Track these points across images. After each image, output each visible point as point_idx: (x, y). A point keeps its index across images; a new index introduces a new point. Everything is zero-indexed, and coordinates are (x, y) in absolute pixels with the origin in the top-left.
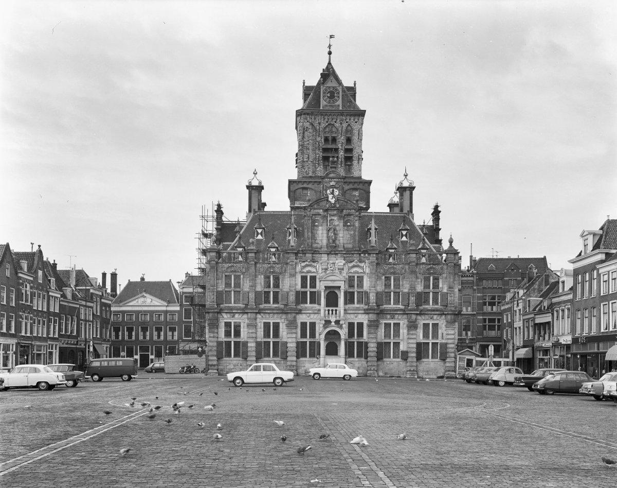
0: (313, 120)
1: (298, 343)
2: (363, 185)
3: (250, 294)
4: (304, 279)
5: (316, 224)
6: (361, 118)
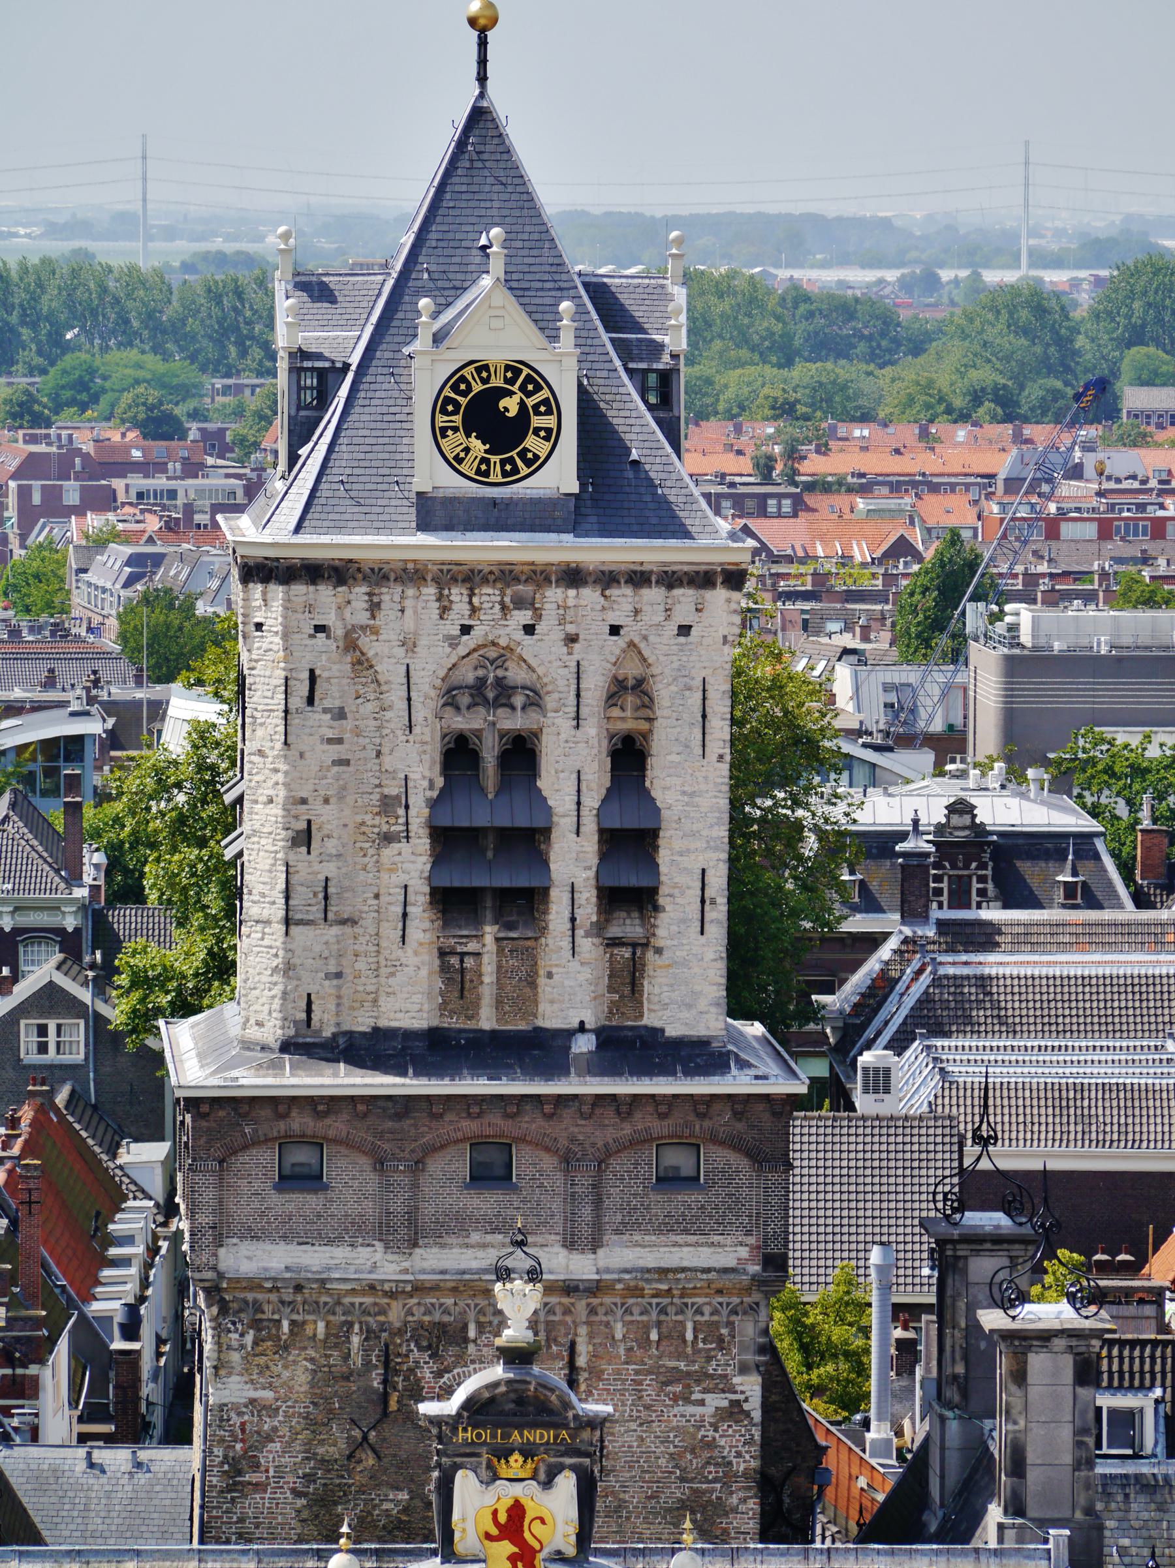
0: (363, 618)
2: (737, 1115)
6: (719, 596)
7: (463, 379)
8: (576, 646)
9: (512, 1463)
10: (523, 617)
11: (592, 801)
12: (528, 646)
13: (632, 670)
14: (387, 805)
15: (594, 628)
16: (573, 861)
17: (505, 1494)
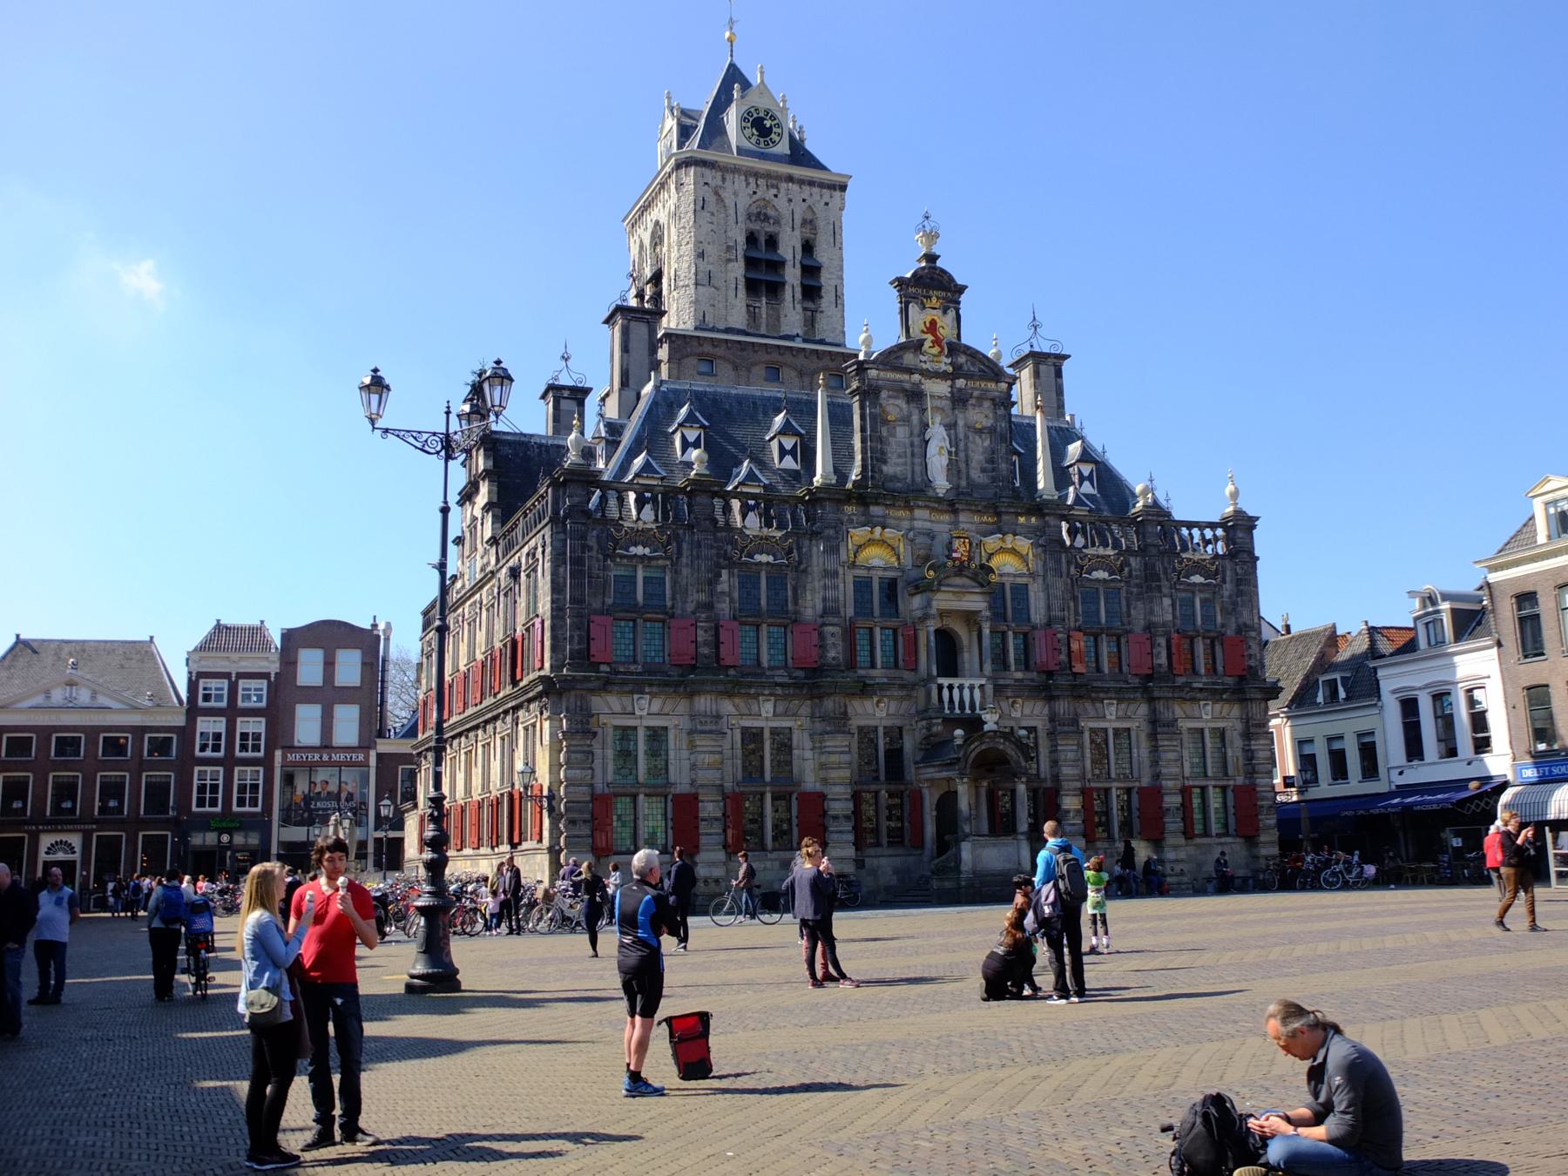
1: (856, 797)
3: (700, 632)
4: (862, 586)
6: (837, 194)
10: (774, 191)
11: (799, 257)
13: (809, 216)
14: (729, 248)
16: (792, 275)
17: (929, 315)
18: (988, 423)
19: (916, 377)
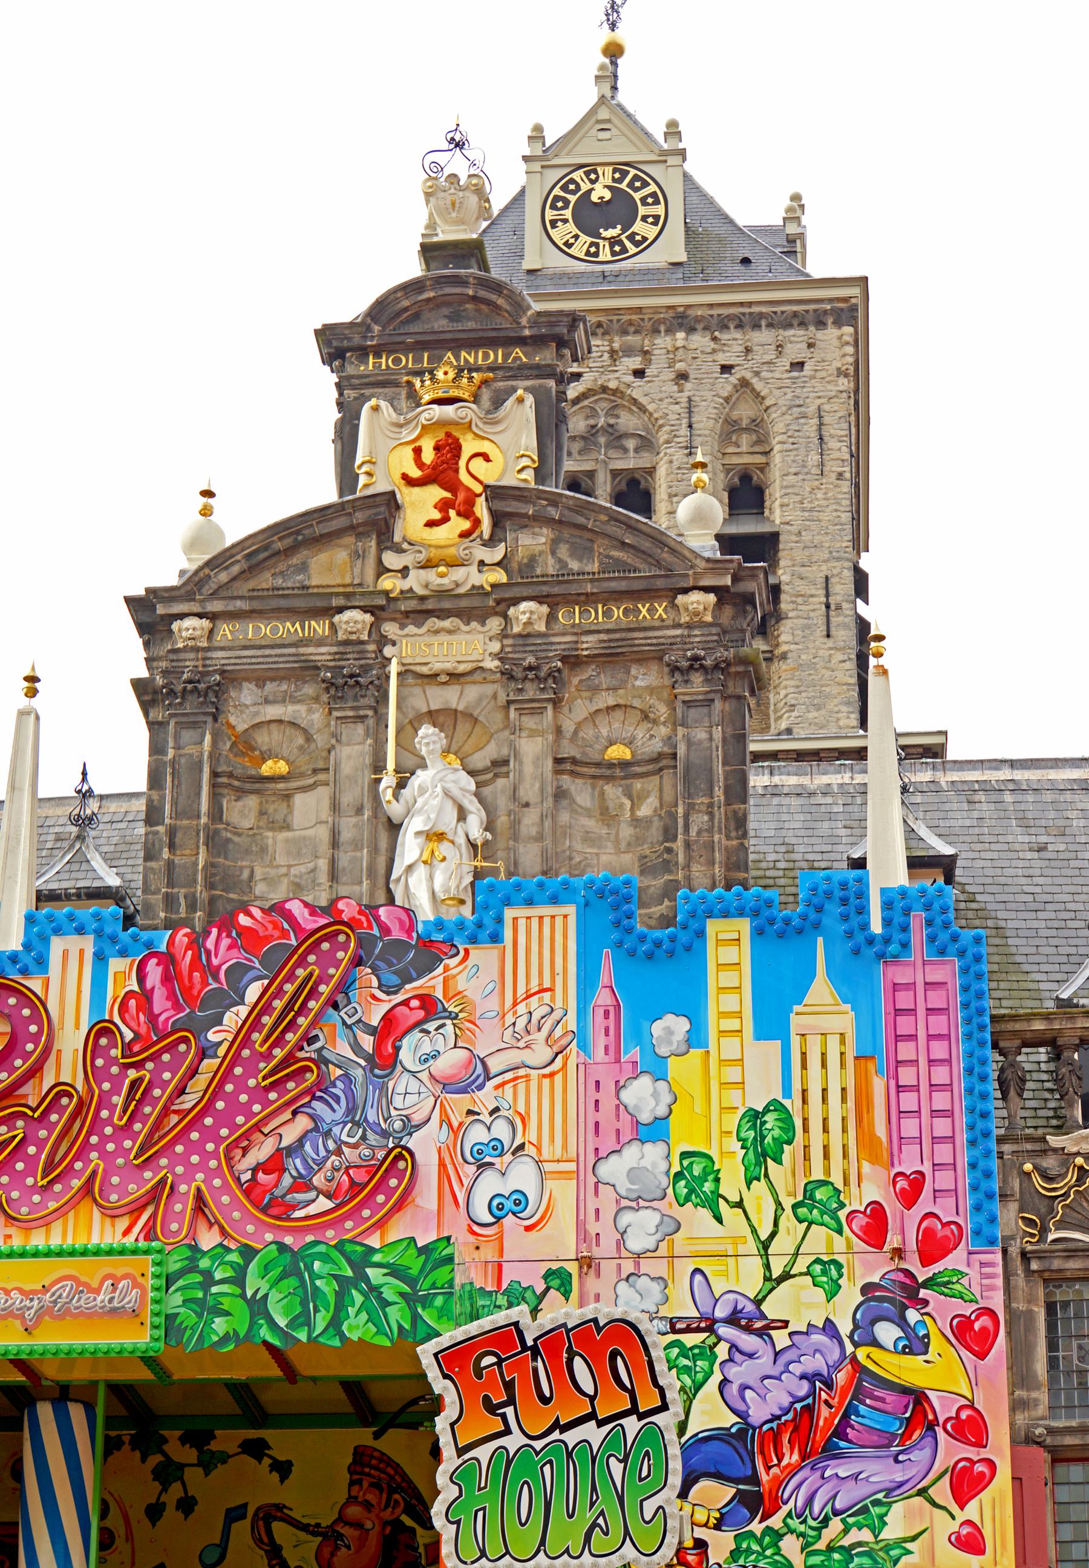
5: (268, 768)
6: (833, 339)
7: (572, 181)
8: (688, 386)
9: (440, 375)
12: (638, 390)
13: (745, 412)
15: (705, 368)
18: (651, 741)
19: (354, 621)
